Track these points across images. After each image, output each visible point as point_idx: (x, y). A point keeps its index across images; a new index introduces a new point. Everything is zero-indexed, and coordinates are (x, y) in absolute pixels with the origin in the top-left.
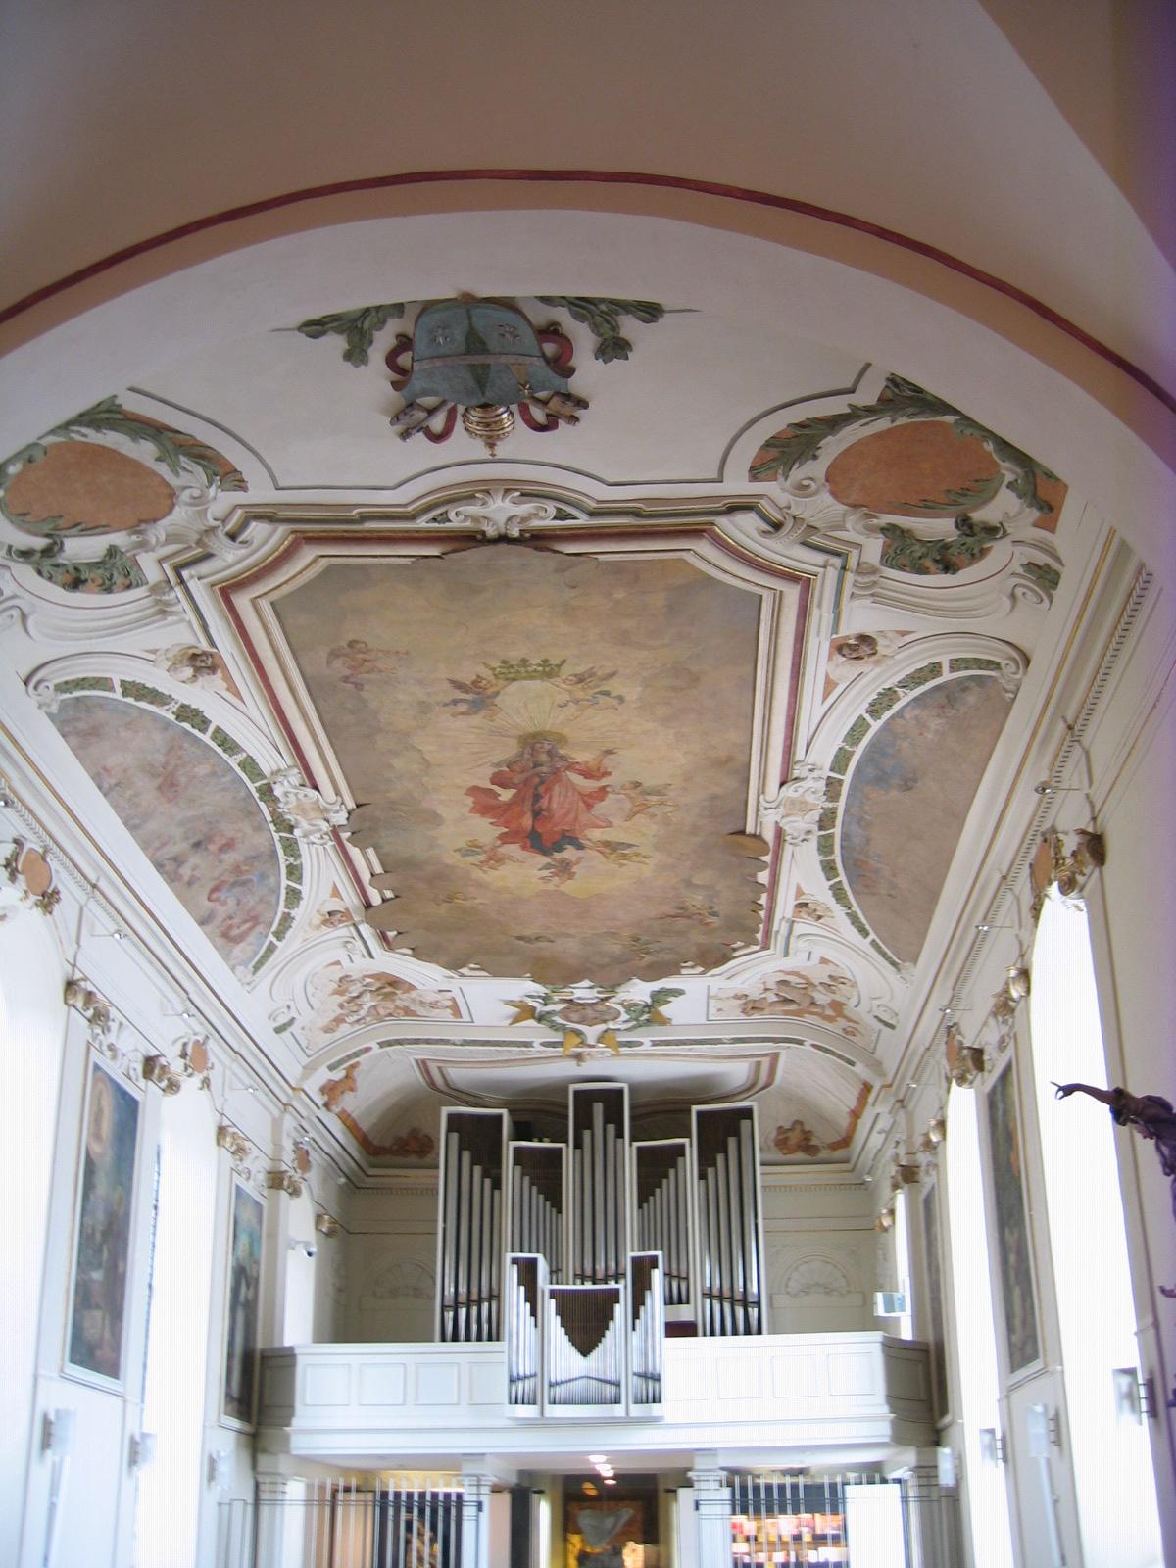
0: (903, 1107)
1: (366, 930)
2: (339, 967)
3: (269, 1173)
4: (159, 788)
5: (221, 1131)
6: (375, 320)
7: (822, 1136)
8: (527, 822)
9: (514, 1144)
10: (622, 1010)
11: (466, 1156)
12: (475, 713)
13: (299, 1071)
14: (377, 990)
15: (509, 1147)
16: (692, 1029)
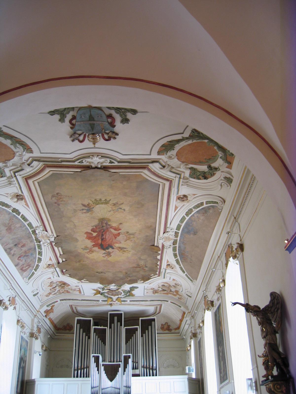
0: (193, 318)
1: (58, 269)
2: (51, 279)
3: (30, 333)
4: (7, 230)
5: (18, 321)
6: (67, 111)
7: (173, 326)
8: (100, 241)
9: (94, 327)
10: (123, 292)
11: (81, 330)
12: (88, 213)
13: (39, 307)
14: (60, 285)
15: (93, 328)
16: (140, 297)
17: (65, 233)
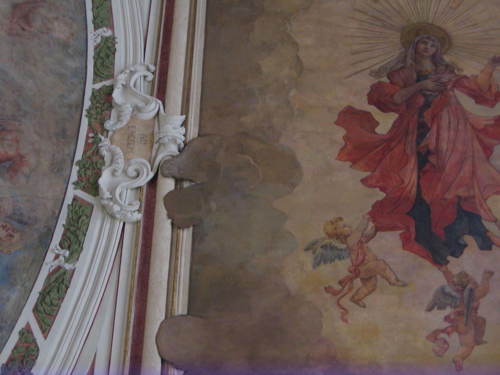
17: (243, 119)
